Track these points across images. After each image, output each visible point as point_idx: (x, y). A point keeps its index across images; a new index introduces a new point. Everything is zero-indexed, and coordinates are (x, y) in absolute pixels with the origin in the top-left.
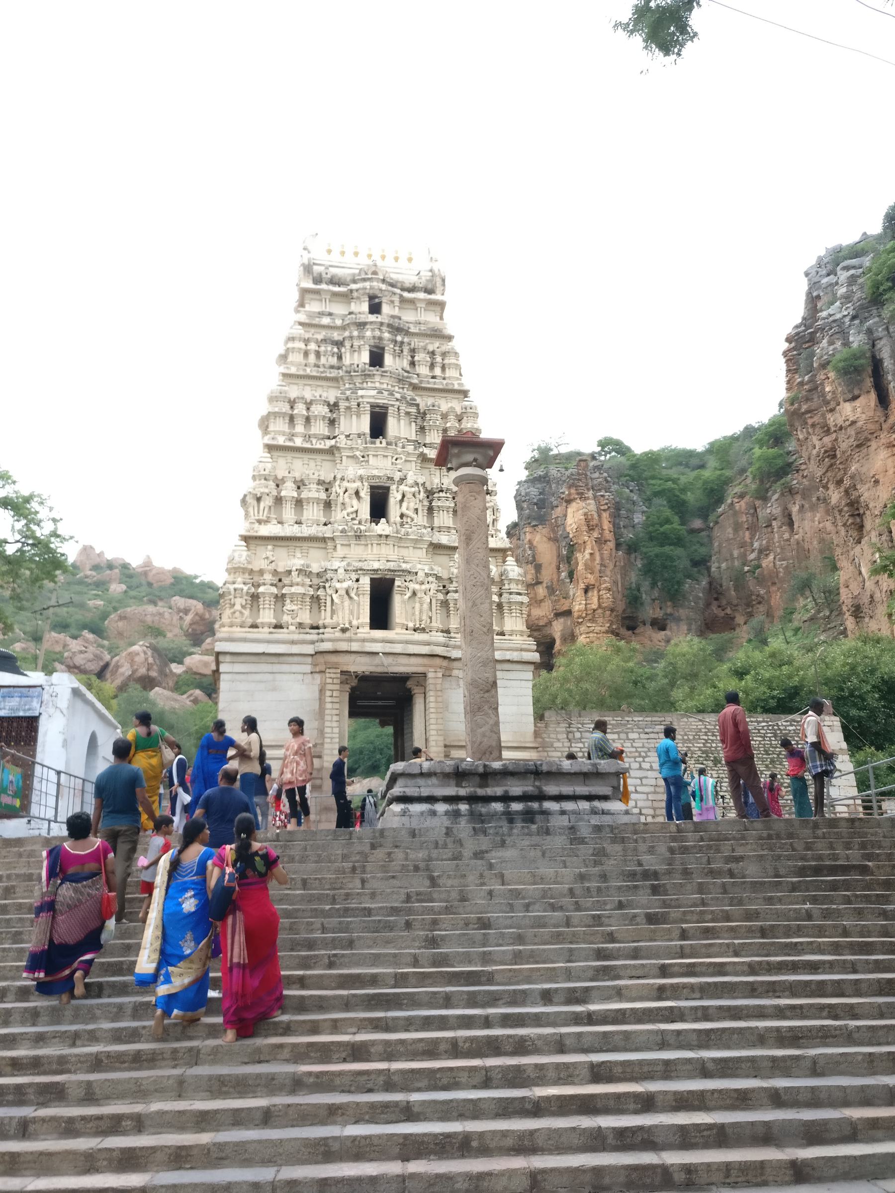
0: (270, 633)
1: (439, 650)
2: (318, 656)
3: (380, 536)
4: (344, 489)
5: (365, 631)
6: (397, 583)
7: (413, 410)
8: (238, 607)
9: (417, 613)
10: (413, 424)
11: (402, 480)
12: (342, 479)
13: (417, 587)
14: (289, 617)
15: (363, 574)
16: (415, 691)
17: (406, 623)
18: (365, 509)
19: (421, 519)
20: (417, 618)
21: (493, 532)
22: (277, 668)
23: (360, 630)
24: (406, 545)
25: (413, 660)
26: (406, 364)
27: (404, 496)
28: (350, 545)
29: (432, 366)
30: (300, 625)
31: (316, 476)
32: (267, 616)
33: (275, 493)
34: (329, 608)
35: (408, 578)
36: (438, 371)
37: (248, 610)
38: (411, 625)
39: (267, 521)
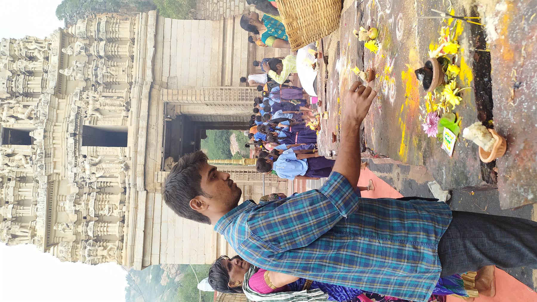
1: (146, 91)
2: (148, 188)
3: (45, 137)
5: (128, 150)
6: (87, 124)
8: (105, 253)
9: (114, 108)
13: (90, 107)
14: (114, 211)
16: (179, 112)
17: (122, 118)
18: (22, 150)
19: (33, 103)
21: (47, 43)
22: (157, 221)
24: (55, 116)
27: (12, 116)
28: (55, 162)
30: (122, 202)
32: (114, 229)
33: (9, 223)
34: (109, 180)
35: (83, 114)
37: (108, 244)
38: (124, 113)
39: (34, 229)
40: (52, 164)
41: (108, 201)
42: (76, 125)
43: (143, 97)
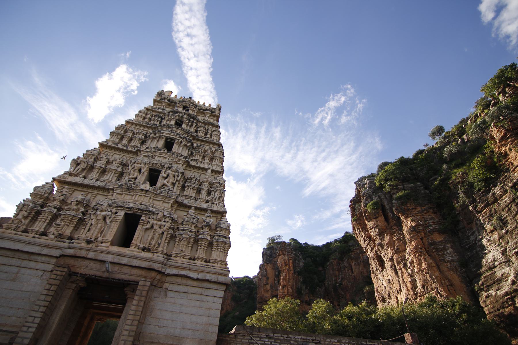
0: (34, 237)
1: (156, 266)
3: (142, 190)
4: (133, 167)
6: (143, 218)
7: (189, 144)
9: (149, 239)
10: (187, 150)
11: (169, 168)
12: (134, 163)
15: (121, 210)
17: (139, 244)
20: (148, 242)
21: (217, 203)
22: (25, 263)
23: (103, 245)
25: (134, 271)
26: (192, 130)
27: (168, 176)
29: (206, 134)
30: (60, 236)
31: (121, 161)
34: (87, 228)
35: (151, 217)
36: (208, 136)
38: (142, 246)
40: (121, 193)
41: (68, 226)
42: (144, 210)
43: (151, 263)
